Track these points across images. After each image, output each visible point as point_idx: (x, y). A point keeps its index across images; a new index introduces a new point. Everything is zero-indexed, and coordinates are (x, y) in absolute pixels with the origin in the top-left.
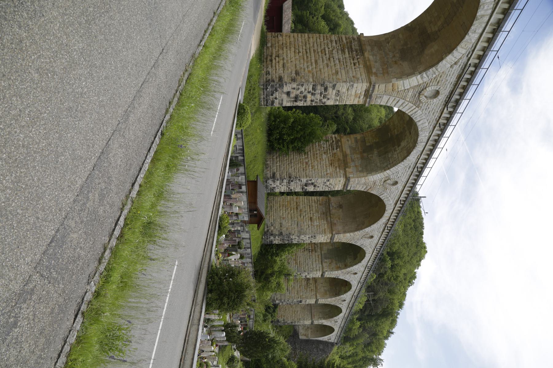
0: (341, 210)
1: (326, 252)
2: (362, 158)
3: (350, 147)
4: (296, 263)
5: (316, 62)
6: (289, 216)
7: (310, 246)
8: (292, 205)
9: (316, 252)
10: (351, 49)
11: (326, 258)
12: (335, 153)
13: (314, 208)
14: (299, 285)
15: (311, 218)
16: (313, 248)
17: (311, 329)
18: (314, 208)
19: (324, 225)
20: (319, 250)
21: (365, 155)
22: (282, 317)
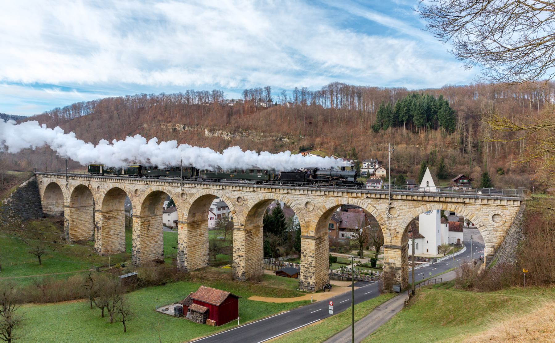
0: (196, 214)
1: (149, 213)
2: (256, 217)
3: (251, 224)
4: (157, 235)
5: (324, 260)
6: (199, 250)
7: (146, 226)
8: (193, 250)
9: (149, 221)
10: (319, 244)
11: (154, 213)
12: (253, 234)
13: (194, 234)
14: (114, 225)
15: (200, 235)
16: (147, 223)
17: (57, 199)
18: (194, 234)
19: (203, 226)
20: (149, 218)
21: (256, 215)
22: (90, 232)
